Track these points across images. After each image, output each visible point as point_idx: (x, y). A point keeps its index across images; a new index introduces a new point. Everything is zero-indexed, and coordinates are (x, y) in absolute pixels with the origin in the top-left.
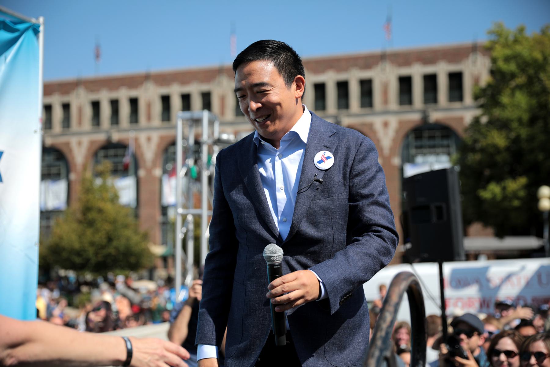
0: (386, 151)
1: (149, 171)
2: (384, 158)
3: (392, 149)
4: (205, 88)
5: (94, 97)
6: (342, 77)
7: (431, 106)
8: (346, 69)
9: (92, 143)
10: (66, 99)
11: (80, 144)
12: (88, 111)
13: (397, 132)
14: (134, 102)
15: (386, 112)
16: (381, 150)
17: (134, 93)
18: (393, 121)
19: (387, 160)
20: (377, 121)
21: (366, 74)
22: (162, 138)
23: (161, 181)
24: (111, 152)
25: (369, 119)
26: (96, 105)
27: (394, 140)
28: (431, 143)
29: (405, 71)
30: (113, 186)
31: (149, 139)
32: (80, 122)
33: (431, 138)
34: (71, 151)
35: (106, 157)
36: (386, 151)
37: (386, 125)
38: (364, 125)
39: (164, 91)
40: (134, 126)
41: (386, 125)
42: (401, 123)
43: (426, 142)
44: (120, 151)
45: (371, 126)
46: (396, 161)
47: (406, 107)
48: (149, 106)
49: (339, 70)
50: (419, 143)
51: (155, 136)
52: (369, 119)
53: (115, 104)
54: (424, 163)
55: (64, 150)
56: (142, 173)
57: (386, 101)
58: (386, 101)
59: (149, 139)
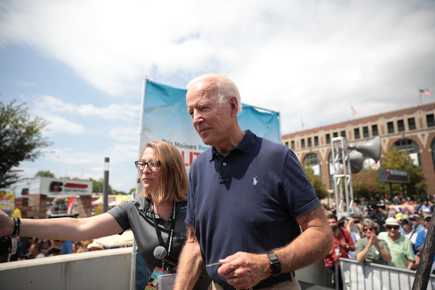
0: (425, 146)
1: (324, 162)
3: (427, 145)
4: (342, 129)
5: (302, 138)
8: (402, 115)
9: (303, 154)
10: (292, 140)
11: (299, 154)
12: (300, 143)
13: (429, 138)
14: (316, 138)
16: (422, 146)
17: (316, 135)
18: (427, 134)
20: (419, 135)
22: (328, 150)
23: (329, 165)
24: (310, 156)
25: (414, 134)
26: (303, 141)
27: (428, 141)
30: (311, 168)
31: (323, 151)
32: (298, 147)
35: (308, 158)
36: (425, 146)
37: (423, 135)
38: (412, 136)
39: (327, 132)
40: (317, 146)
42: (430, 134)
44: (313, 156)
45: (416, 136)
48: (322, 138)
49: (398, 116)
51: (325, 149)
52: (414, 134)
53: (309, 140)
56: (321, 163)
58: (421, 126)
59: (323, 151)
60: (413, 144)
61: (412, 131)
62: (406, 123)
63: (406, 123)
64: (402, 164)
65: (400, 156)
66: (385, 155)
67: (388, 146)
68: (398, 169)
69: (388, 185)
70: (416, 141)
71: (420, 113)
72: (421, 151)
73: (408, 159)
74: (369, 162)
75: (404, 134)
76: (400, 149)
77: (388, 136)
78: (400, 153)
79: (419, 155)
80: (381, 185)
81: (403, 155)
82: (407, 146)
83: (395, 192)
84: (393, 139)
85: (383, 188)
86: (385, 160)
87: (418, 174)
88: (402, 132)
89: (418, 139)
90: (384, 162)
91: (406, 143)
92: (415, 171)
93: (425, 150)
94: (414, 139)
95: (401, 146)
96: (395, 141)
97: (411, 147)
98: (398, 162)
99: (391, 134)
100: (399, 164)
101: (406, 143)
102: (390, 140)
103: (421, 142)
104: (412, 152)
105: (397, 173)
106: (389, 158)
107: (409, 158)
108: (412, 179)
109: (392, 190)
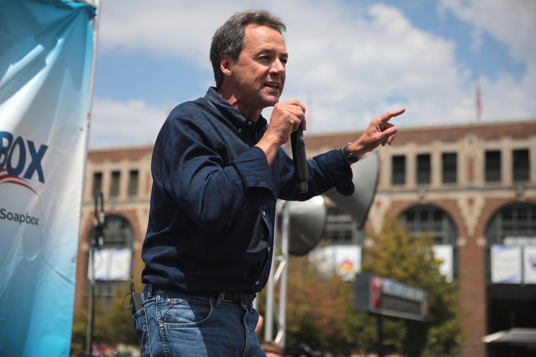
0: (471, 231)
2: (468, 237)
3: (476, 229)
6: (424, 150)
7: (520, 185)
8: (428, 142)
10: (134, 166)
13: (484, 210)
15: (471, 189)
16: (466, 229)
18: (480, 199)
19: (471, 240)
20: (462, 198)
21: (449, 148)
25: (452, 195)
27: (480, 219)
28: (523, 223)
29: (493, 146)
33: (522, 217)
34: (136, 219)
36: (471, 231)
37: (471, 202)
38: (446, 201)
41: (471, 202)
42: (488, 201)
43: (515, 223)
45: (454, 202)
46: (481, 242)
47: (492, 185)
50: (508, 223)
52: (452, 195)
54: (514, 246)
55: (130, 217)
57: (471, 177)
58: (471, 177)
60: (445, 223)
61: (447, 186)
62: (436, 163)
63: (436, 163)
64: (412, 270)
65: (411, 248)
66: (376, 240)
67: (386, 216)
68: (402, 281)
69: (373, 320)
70: (454, 214)
71: (471, 142)
72: (462, 242)
73: (427, 258)
74: (334, 256)
75: (428, 191)
76: (413, 229)
77: (389, 192)
78: (412, 241)
79: (456, 252)
80: (356, 321)
81: (419, 249)
82: (430, 223)
83: (388, 342)
84: (400, 203)
85: (360, 329)
86: (375, 255)
87: (446, 298)
88: (424, 187)
89: (459, 210)
90: (370, 260)
91: (431, 216)
92: (441, 290)
93: (471, 240)
94: (448, 207)
95: (417, 223)
96: (404, 206)
97: (439, 229)
98: (405, 264)
99: (397, 188)
100: (405, 269)
101: (431, 216)
102: (394, 204)
103: (463, 219)
104: (439, 241)
105: (399, 290)
106: (385, 249)
107: (432, 254)
108: (433, 310)
109: (382, 335)
